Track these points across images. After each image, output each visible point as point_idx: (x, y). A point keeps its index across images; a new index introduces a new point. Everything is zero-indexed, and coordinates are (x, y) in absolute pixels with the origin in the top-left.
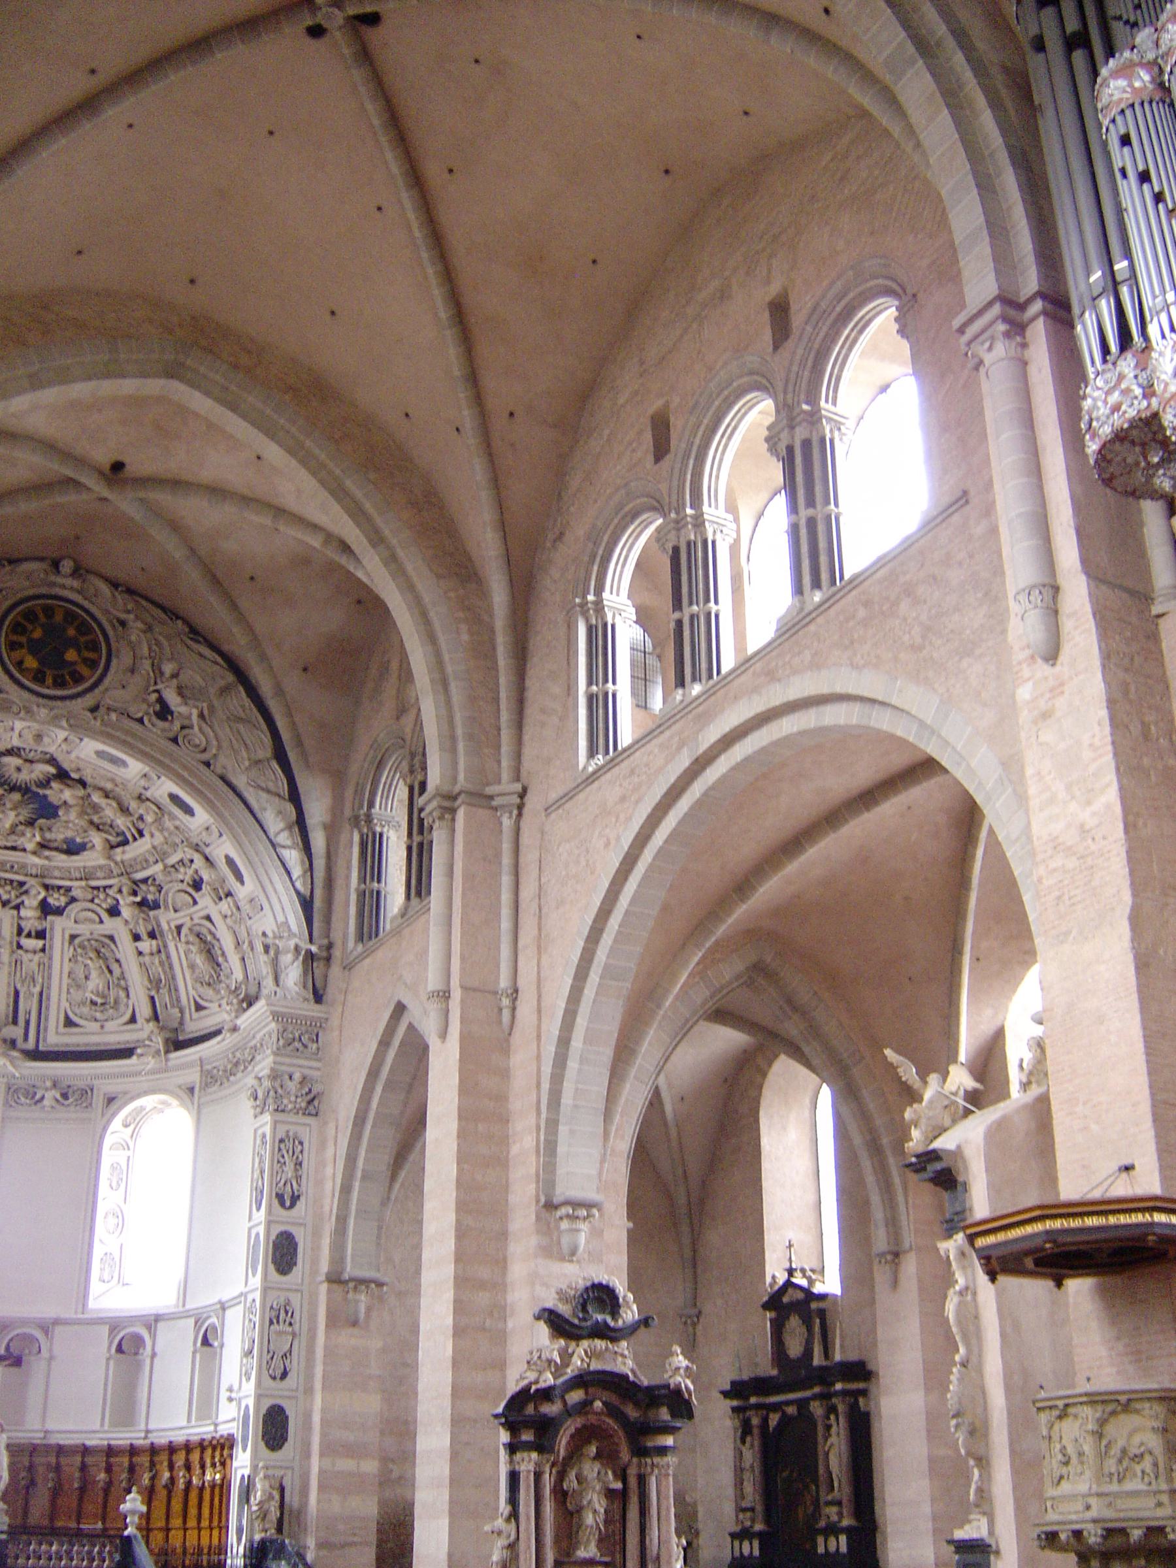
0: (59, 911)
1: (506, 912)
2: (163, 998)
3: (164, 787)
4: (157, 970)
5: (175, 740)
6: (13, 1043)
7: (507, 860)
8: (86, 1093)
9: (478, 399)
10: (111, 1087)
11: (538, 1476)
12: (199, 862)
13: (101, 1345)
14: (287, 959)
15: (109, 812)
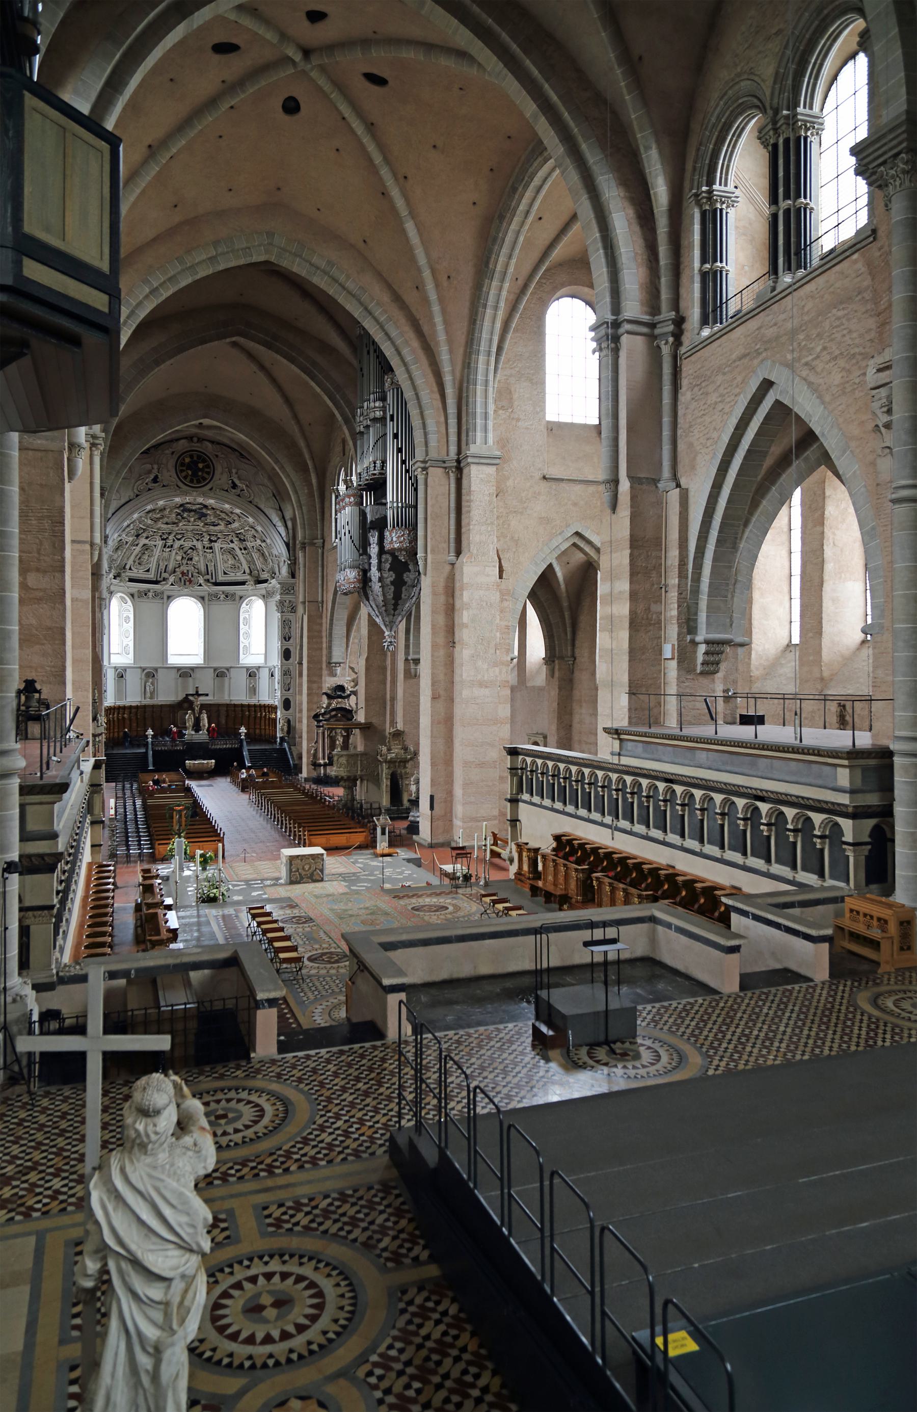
0: (215, 541)
1: (320, 578)
2: (252, 567)
3: (238, 511)
4: (250, 559)
5: (239, 495)
6: (208, 581)
7: (320, 563)
8: (233, 595)
9: (298, 421)
10: (241, 593)
11: (323, 733)
12: (253, 531)
13: (244, 675)
14: (282, 564)
15: (223, 515)
